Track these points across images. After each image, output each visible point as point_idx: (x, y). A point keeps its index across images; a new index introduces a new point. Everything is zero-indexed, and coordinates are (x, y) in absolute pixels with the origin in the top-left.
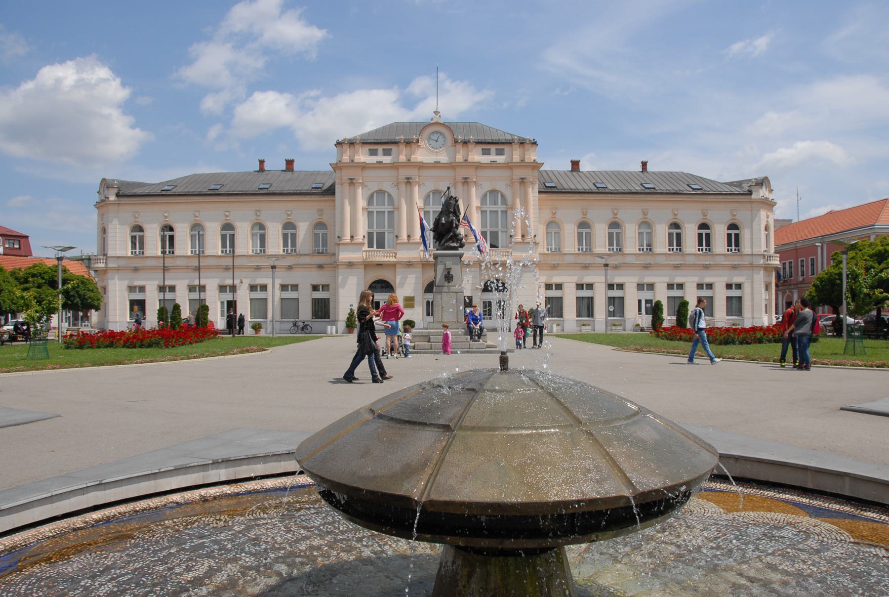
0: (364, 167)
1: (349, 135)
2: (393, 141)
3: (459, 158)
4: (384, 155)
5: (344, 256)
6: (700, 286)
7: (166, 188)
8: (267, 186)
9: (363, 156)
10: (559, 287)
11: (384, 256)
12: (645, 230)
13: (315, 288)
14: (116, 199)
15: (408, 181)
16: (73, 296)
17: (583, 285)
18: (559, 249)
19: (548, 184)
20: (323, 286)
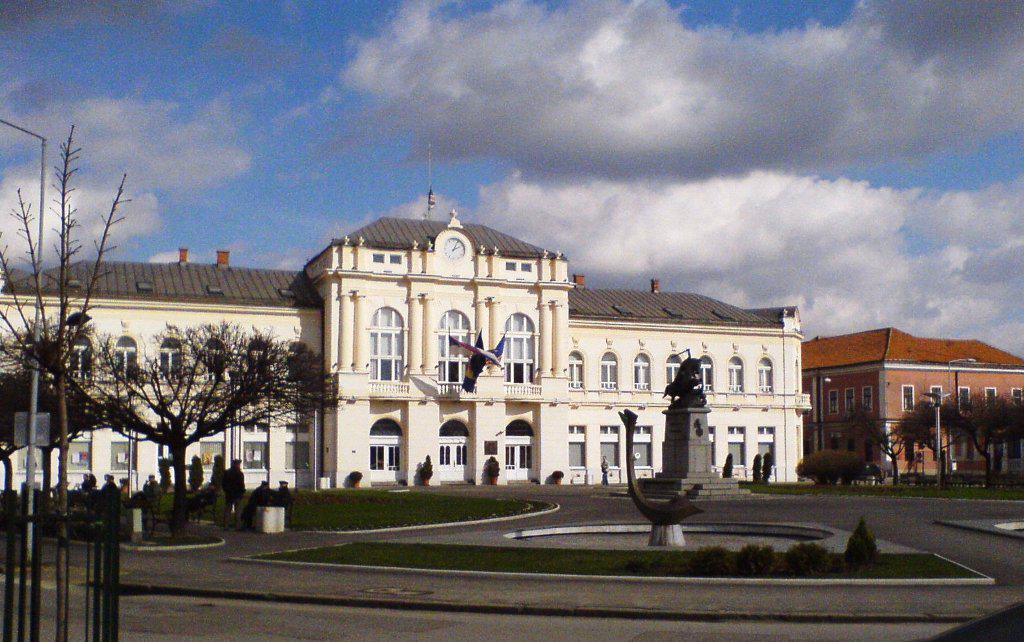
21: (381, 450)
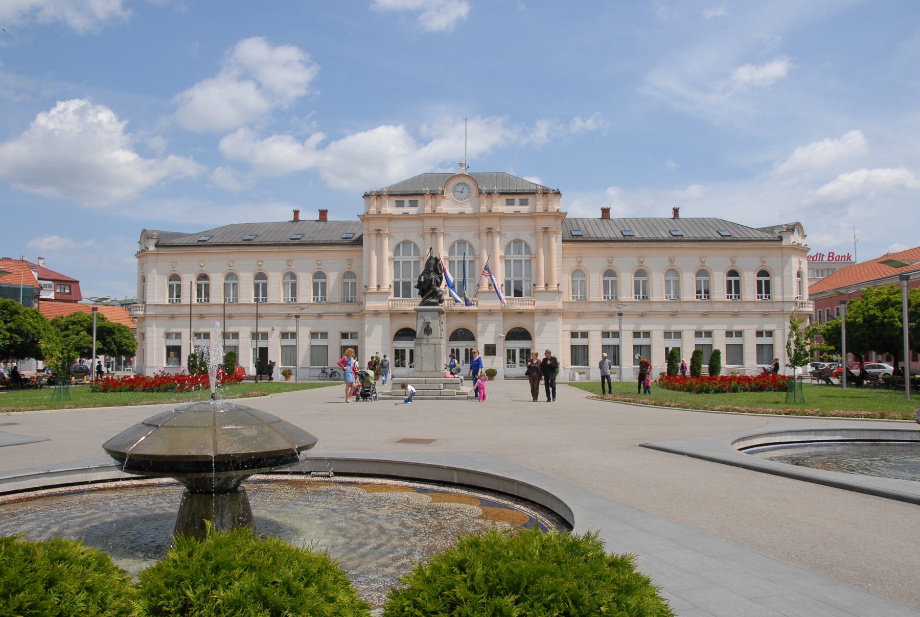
0: (391, 218)
1: (375, 188)
2: (419, 192)
3: (484, 209)
4: (411, 206)
5: (371, 305)
6: (729, 334)
7: (203, 238)
8: (299, 237)
9: (389, 208)
10: (585, 335)
11: (409, 305)
12: (672, 278)
13: (344, 336)
14: (155, 249)
16: (110, 343)
17: (609, 333)
18: (585, 297)
19: (574, 233)
20: (351, 334)
21: (403, 351)
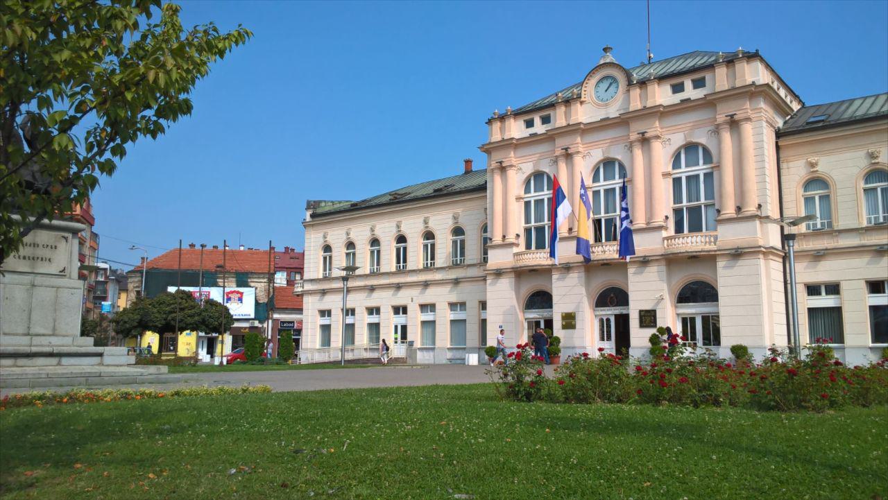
3: (636, 104)
15: (645, 141)
